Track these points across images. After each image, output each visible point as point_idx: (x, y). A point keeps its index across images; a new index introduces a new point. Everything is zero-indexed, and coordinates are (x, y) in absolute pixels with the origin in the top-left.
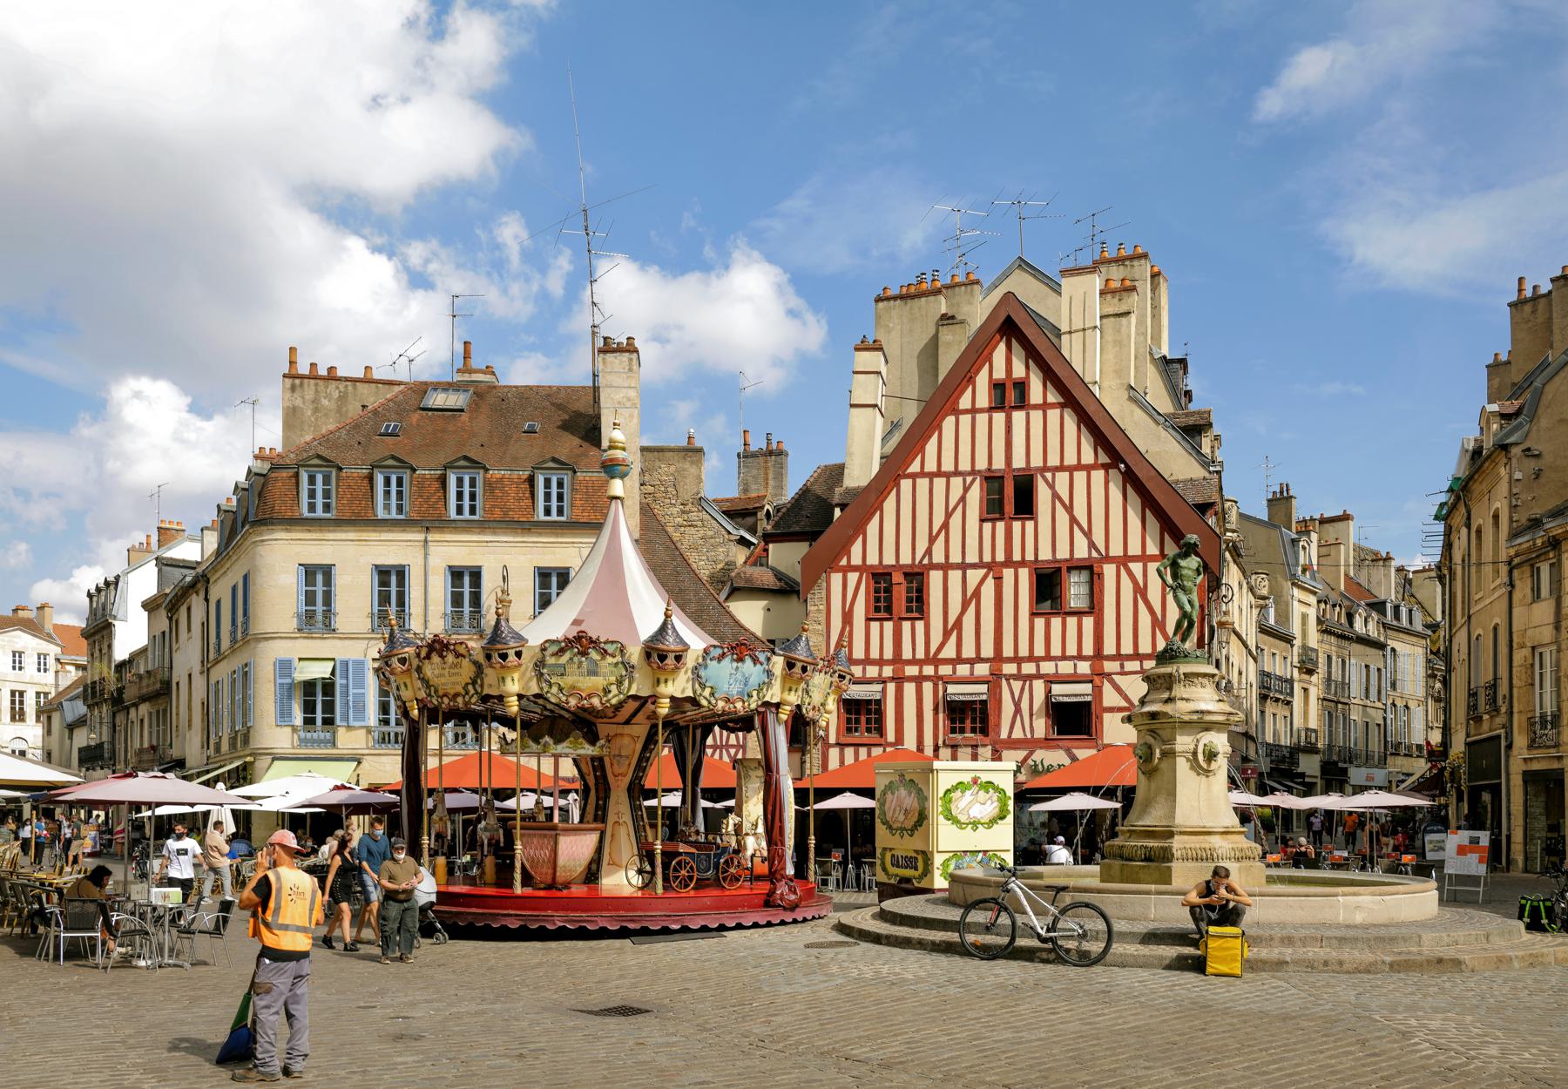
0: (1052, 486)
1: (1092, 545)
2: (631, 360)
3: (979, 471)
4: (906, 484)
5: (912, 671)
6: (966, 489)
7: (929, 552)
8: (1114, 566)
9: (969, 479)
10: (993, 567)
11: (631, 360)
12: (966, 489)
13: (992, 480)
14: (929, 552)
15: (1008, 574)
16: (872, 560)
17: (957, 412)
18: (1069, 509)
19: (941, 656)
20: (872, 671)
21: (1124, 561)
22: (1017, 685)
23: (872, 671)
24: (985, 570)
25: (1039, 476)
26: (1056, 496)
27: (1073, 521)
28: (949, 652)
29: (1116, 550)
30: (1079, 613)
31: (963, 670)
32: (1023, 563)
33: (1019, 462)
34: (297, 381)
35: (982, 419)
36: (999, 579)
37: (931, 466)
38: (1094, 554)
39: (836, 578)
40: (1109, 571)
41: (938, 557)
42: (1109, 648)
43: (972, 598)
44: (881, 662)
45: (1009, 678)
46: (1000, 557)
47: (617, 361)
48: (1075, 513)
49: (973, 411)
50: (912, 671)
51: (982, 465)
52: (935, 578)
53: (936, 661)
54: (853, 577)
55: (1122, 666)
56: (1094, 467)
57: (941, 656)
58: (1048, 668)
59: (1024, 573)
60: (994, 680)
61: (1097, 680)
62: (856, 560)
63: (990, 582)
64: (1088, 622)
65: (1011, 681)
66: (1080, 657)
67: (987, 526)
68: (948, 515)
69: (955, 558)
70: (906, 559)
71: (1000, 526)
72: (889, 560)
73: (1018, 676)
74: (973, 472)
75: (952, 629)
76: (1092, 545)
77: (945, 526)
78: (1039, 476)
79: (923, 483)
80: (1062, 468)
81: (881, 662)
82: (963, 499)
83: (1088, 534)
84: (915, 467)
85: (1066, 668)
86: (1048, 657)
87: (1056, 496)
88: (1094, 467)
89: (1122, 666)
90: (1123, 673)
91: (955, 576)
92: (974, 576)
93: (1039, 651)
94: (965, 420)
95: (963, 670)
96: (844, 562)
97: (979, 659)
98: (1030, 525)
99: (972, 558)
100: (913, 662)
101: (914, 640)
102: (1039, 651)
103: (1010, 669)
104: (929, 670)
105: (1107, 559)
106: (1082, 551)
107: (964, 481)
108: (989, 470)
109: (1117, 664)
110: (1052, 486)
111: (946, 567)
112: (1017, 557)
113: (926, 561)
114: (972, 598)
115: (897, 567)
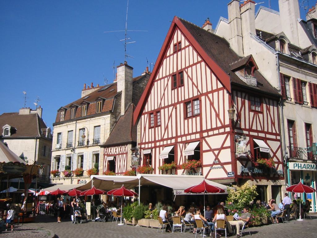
0: (187, 73)
1: (198, 91)
2: (123, 67)
3: (171, 74)
4: (156, 83)
5: (158, 144)
6: (168, 81)
7: (161, 104)
8: (204, 96)
9: (169, 77)
10: (174, 105)
11: (123, 67)
12: (168, 81)
13: (174, 76)
14: (161, 104)
15: (178, 106)
16: (150, 110)
17: (166, 57)
18: (192, 80)
19: (164, 138)
20: (150, 145)
21: (206, 94)
22: (181, 145)
23: (150, 145)
24: (173, 107)
25: (184, 71)
26: (188, 76)
27: (193, 83)
28: (166, 137)
29: (205, 91)
30: (196, 116)
31: (169, 142)
32: (181, 102)
33: (179, 68)
34: (84, 91)
35: (172, 57)
36: (176, 108)
37: (161, 77)
38: (199, 94)
39: (143, 116)
40: (203, 98)
41: (163, 106)
42: (204, 129)
43: (170, 116)
44: (151, 142)
45: (179, 143)
46: (176, 101)
47: (120, 69)
48: (193, 81)
49: (169, 56)
50: (158, 144)
51: (171, 72)
52: (162, 111)
53: (163, 140)
54: (146, 115)
55: (208, 134)
56: (198, 63)
57: (164, 138)
58: (188, 138)
59: (182, 105)
60: (175, 145)
61: (201, 139)
62: (146, 111)
63: (174, 109)
64: (198, 118)
65: (180, 144)
66: (197, 133)
67: (173, 91)
68: (165, 90)
69: (166, 105)
70: (156, 108)
71: (176, 90)
72: (153, 109)
73: (182, 142)
74: (170, 75)
75: (166, 128)
76: (198, 91)
77: (164, 94)
78: (184, 71)
79: (159, 82)
80: (190, 66)
81: (151, 142)
82: (167, 84)
83: (197, 87)
84: (157, 78)
85: (193, 137)
86: (189, 134)
87: (188, 76)
88: (198, 63)
89: (208, 134)
90: (208, 136)
91: (166, 109)
92: (171, 108)
93: (186, 133)
94: (168, 59)
95: (169, 142)
96: (144, 112)
97: (172, 138)
98: (183, 88)
99: (170, 103)
100: (159, 141)
101: (159, 133)
102: (186, 133)
103: (179, 140)
104: (162, 143)
105: (202, 94)
106: (195, 94)
107: (168, 78)
108: (173, 73)
109: (206, 133)
110: (187, 73)
111: (164, 108)
112: (180, 100)
113: (160, 107)
114: (170, 116)
115: (154, 110)
